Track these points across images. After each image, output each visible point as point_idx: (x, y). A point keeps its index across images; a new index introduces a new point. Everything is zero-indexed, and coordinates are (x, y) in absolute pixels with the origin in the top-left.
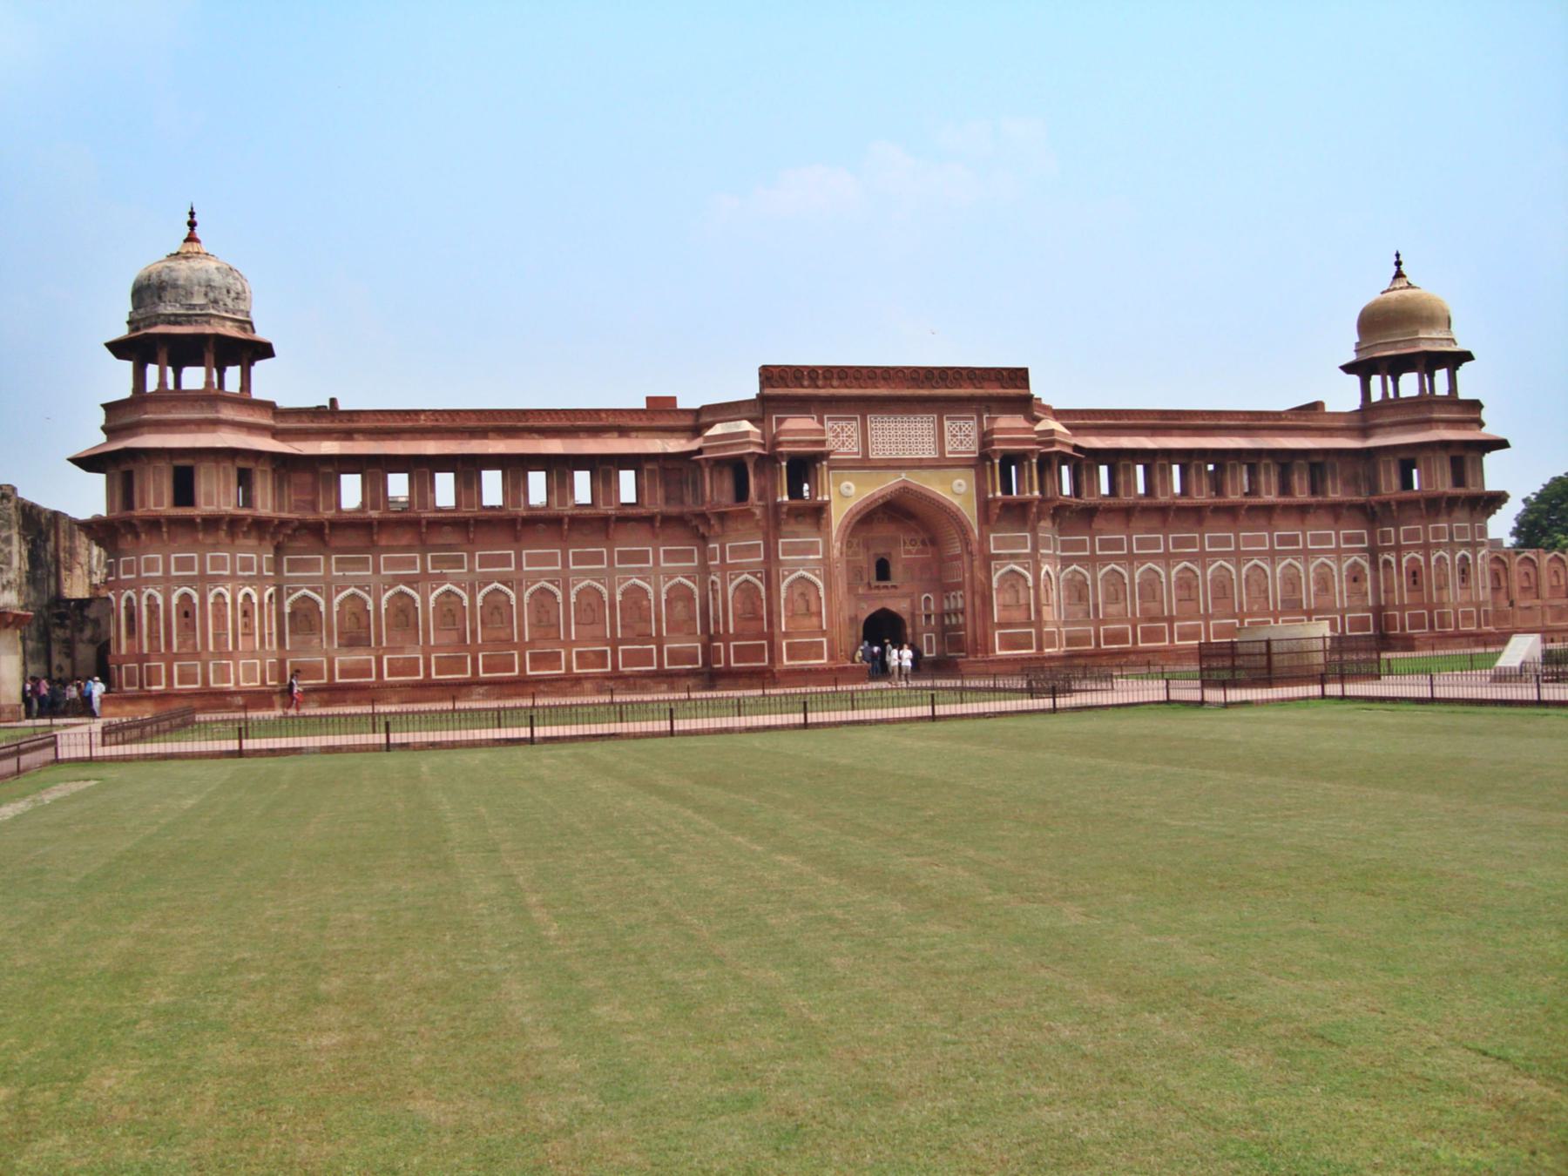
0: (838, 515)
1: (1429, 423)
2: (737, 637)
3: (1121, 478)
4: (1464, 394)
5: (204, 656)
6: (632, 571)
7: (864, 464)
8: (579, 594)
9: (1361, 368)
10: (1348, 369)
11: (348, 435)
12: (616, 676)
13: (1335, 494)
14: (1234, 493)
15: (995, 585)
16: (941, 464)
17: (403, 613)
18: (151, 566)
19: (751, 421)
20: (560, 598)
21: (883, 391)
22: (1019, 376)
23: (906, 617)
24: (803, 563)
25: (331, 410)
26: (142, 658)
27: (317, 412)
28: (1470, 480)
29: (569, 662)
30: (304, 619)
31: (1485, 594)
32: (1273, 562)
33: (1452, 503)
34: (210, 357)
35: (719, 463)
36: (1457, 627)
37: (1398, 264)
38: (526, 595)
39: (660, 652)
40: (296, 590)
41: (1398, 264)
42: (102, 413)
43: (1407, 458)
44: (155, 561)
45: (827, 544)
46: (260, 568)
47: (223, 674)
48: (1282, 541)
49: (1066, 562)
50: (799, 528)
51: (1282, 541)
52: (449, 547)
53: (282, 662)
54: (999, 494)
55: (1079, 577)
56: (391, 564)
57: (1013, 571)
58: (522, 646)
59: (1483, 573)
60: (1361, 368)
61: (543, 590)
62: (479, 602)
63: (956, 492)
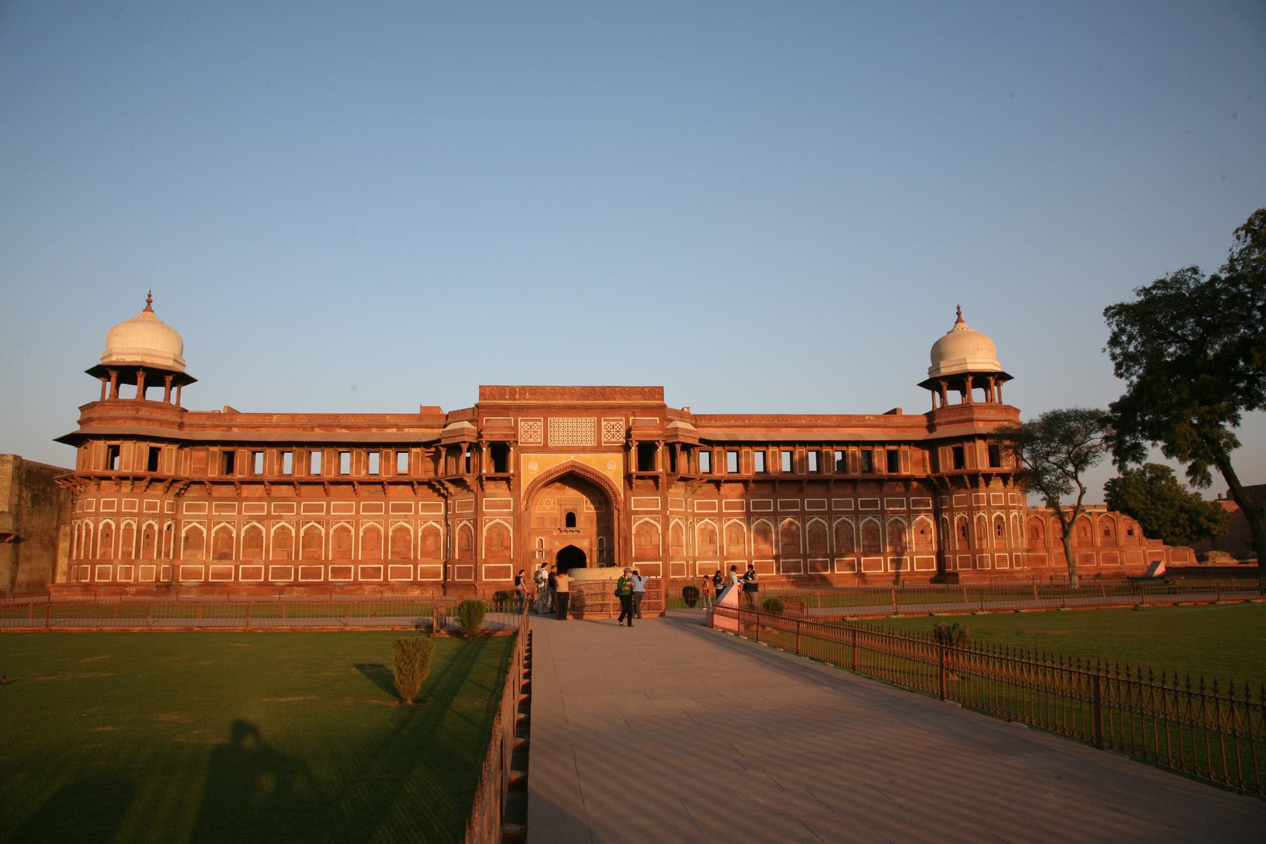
0: (525, 483)
1: (971, 420)
2: (459, 561)
3: (743, 461)
4: (1004, 403)
5: (115, 562)
6: (400, 517)
7: (545, 449)
8: (365, 532)
9: (934, 384)
10: (924, 385)
11: (230, 428)
12: (386, 584)
13: (906, 470)
14: (828, 471)
15: (634, 532)
16: (599, 449)
17: (254, 539)
18: (89, 505)
19: (470, 421)
20: (353, 533)
21: (561, 402)
22: (658, 392)
23: (586, 552)
24: (499, 514)
25: (232, 412)
26: (79, 562)
27: (211, 415)
28: (1003, 463)
29: (356, 574)
30: (194, 540)
31: (1024, 542)
32: (857, 519)
33: (988, 477)
34: (141, 380)
35: (454, 449)
36: (993, 566)
37: (959, 314)
38: (331, 531)
39: (415, 569)
40: (189, 523)
41: (959, 314)
42: (79, 413)
43: (959, 445)
44: (90, 504)
45: (517, 502)
46: (162, 509)
47: (127, 573)
48: (864, 504)
49: (701, 517)
50: (499, 491)
51: (864, 504)
52: (285, 499)
53: (174, 568)
54: (634, 470)
55: (710, 527)
56: (249, 508)
57: (647, 522)
58: (326, 562)
59: (1015, 528)
60: (934, 384)
61: (343, 529)
62: (302, 534)
63: (611, 468)
